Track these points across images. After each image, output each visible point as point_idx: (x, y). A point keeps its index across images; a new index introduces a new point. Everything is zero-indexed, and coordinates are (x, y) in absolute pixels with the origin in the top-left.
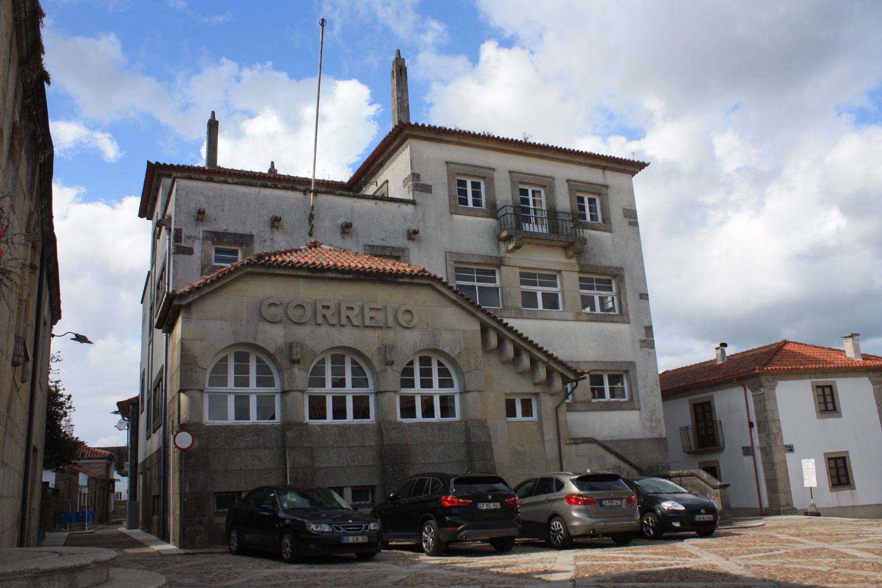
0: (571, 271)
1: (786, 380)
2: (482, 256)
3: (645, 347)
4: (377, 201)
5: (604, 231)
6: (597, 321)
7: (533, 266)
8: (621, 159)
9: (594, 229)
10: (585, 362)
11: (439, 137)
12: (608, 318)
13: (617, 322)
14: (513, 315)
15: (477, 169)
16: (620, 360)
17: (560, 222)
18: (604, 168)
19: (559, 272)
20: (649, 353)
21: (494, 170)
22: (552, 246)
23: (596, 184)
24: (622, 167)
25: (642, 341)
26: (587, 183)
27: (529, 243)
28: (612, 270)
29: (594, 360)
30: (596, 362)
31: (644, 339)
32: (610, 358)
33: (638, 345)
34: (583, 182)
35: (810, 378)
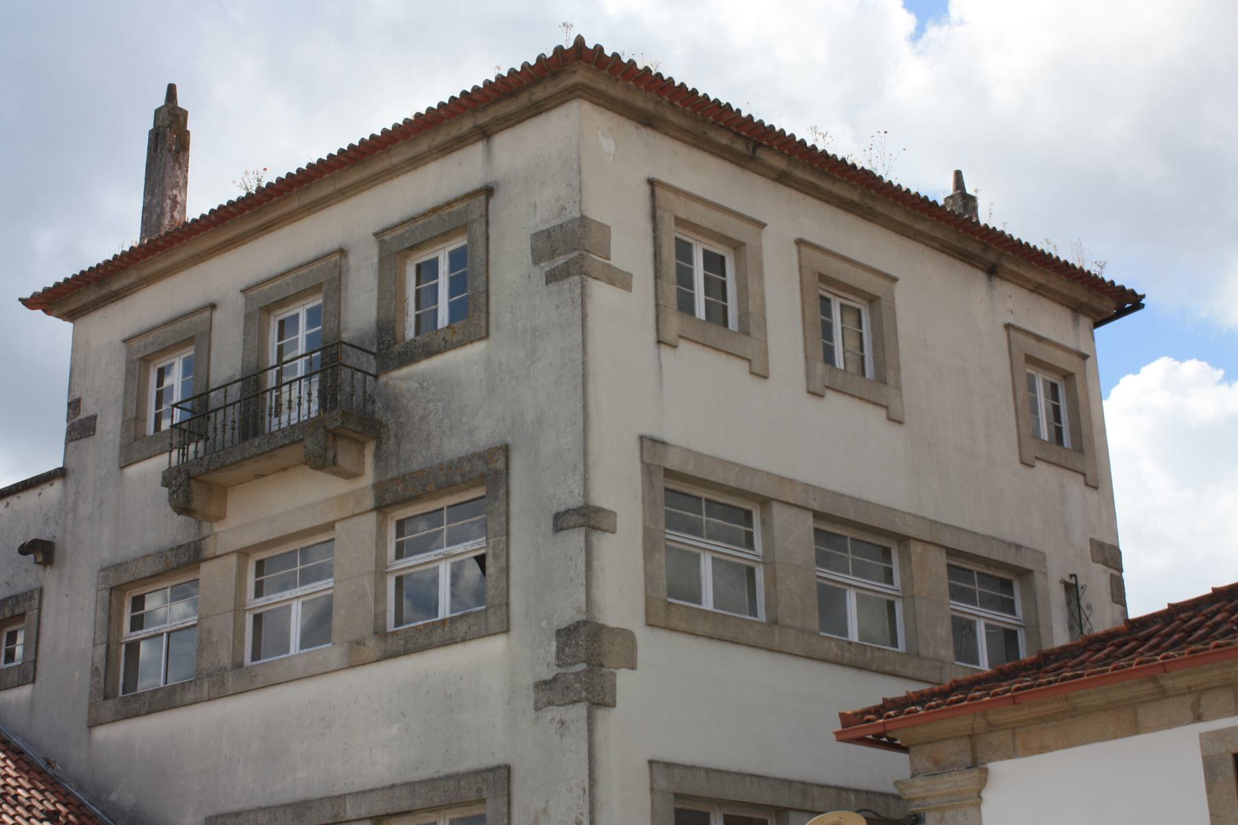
0: (355, 515)
1: (1043, 749)
2: (160, 554)
3: (550, 703)
4: (9, 500)
5: (461, 344)
6: (406, 652)
7: (263, 539)
8: (488, 84)
9: (430, 354)
10: (357, 793)
11: (105, 291)
12: (438, 635)
13: (464, 640)
14: (205, 695)
15: (178, 325)
16: (462, 767)
17: (345, 374)
18: (485, 134)
19: (330, 526)
20: (562, 723)
21: (213, 306)
22: (284, 469)
23: (449, 204)
24: (523, 100)
25: (543, 685)
26: (425, 214)
27: (260, 476)
28: (467, 467)
29: (388, 783)
30: (393, 786)
31: (549, 677)
32: (437, 767)
33: (526, 702)
34: (413, 219)
35: (1198, 718)
